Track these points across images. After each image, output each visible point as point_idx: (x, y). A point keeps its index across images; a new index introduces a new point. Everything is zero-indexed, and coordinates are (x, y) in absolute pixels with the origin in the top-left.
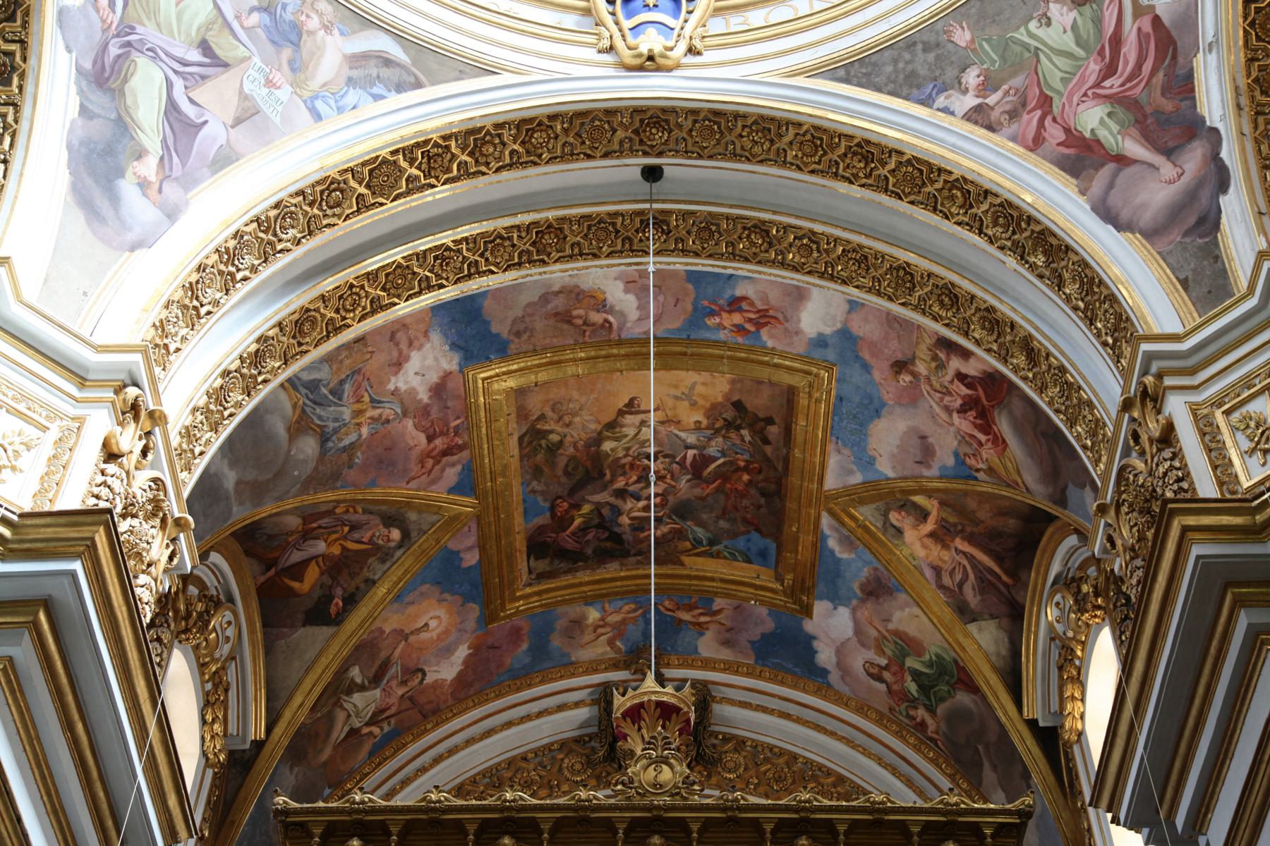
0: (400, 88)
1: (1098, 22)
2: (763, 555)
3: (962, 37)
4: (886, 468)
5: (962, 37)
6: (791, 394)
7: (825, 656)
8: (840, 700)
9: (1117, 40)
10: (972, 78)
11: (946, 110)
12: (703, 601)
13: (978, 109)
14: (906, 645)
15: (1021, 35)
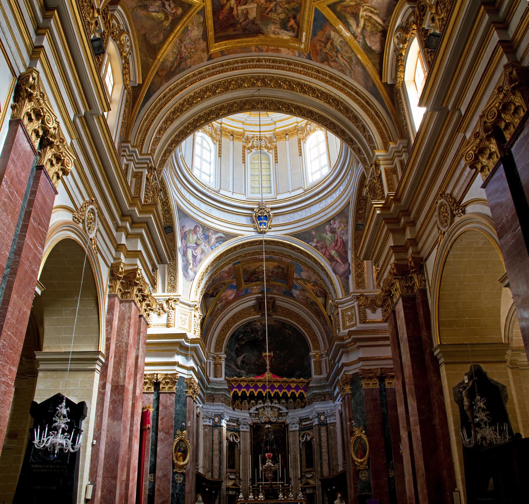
0: (224, 241)
1: (334, 237)
2: (284, 283)
3: (314, 233)
4: (304, 277)
5: (314, 233)
6: (288, 267)
7: (295, 295)
8: (297, 301)
9: (337, 241)
10: (315, 240)
11: (311, 245)
12: (274, 286)
13: (316, 246)
14: (308, 298)
15: (323, 235)
